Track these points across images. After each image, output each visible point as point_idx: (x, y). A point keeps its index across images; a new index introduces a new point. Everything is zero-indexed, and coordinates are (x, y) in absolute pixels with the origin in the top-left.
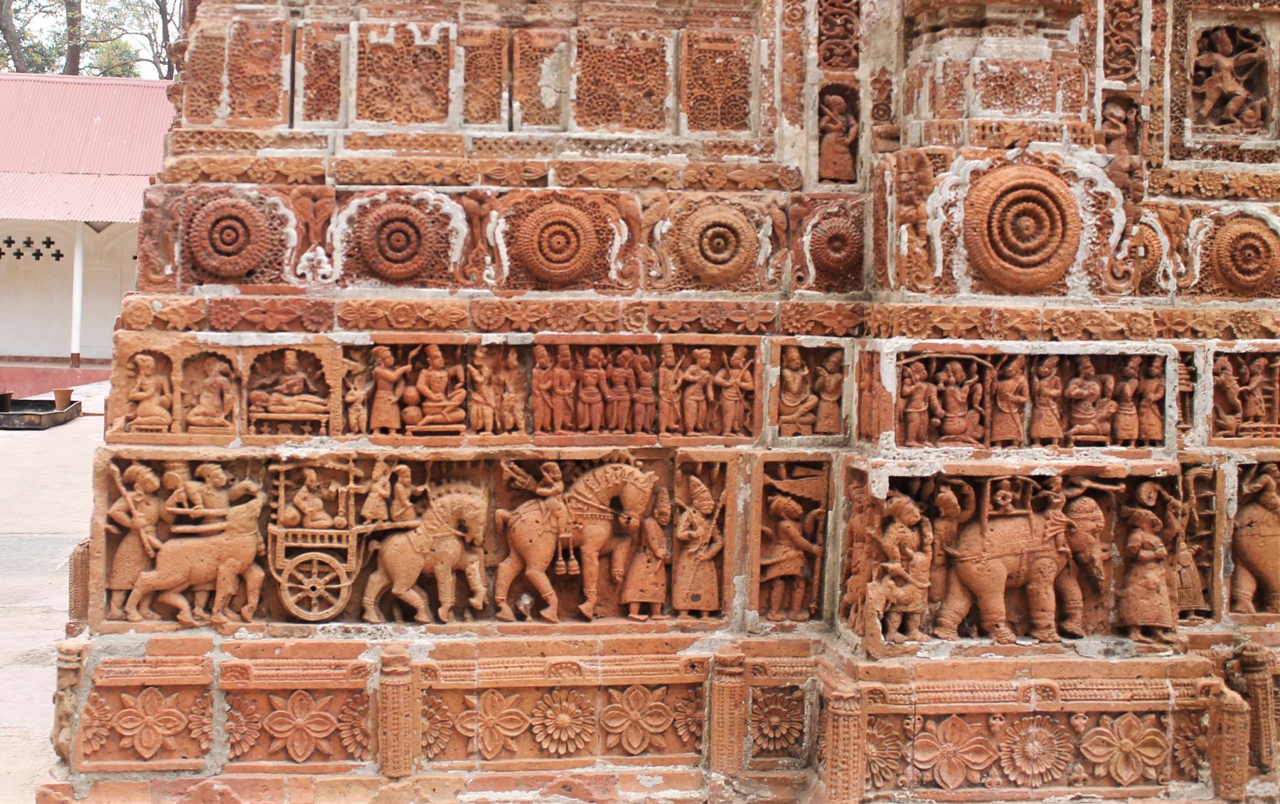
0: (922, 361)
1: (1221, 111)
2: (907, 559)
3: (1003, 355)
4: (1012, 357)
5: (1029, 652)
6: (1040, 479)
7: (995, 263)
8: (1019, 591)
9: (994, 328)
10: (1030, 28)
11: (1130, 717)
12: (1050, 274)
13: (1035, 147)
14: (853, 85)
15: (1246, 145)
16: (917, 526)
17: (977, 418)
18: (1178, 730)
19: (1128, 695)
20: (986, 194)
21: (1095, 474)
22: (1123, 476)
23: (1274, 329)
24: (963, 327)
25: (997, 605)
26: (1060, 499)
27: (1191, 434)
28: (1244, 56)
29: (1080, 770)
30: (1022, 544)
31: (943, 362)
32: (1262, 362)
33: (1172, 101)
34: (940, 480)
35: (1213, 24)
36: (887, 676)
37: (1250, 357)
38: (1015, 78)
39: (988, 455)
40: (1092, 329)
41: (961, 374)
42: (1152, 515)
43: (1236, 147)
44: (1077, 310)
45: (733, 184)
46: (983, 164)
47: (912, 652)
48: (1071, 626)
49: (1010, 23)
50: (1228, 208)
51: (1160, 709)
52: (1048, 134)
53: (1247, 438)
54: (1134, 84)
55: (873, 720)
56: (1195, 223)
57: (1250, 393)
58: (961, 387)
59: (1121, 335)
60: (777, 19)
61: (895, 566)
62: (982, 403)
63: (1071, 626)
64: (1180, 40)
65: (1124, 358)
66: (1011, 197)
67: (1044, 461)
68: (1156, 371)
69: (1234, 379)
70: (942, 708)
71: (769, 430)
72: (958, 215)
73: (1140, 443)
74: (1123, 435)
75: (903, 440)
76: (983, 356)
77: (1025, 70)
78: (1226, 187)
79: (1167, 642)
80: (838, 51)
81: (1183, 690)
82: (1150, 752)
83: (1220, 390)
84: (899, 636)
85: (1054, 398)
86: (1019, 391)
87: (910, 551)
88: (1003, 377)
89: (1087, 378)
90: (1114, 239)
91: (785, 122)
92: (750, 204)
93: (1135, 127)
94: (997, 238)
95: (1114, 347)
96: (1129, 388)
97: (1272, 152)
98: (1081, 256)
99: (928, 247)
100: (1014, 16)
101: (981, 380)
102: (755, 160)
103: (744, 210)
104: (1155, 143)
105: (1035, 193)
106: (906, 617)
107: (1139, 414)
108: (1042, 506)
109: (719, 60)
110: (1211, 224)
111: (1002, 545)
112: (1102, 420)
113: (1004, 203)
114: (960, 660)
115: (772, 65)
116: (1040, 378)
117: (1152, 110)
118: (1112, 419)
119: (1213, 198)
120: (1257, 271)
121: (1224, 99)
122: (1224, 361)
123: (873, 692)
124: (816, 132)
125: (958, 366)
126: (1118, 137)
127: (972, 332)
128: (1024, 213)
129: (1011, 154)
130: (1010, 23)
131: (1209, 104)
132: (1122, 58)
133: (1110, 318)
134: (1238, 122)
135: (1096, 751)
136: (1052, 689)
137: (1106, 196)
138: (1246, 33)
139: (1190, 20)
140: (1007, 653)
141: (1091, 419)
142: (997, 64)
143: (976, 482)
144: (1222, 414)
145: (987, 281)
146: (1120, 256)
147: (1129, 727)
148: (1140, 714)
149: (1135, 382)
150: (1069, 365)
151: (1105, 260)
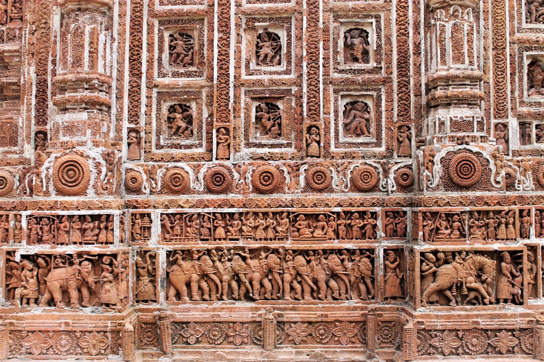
0: (34, 218)
1: (178, 132)
2: (27, 281)
3: (60, 215)
4: (63, 216)
5: (67, 312)
6: (71, 255)
7: (61, 186)
8: (65, 291)
9: (59, 207)
10: (81, 110)
11: (95, 333)
12: (79, 189)
13: (78, 148)
14: (45, 131)
15: (183, 143)
16: (31, 270)
17: (52, 236)
18: (112, 338)
19: (95, 325)
20: (57, 164)
21: (88, 253)
22: (96, 254)
23: (183, 205)
24: (48, 207)
25: (58, 296)
26: (78, 261)
27: (151, 241)
28: (185, 113)
29: (79, 350)
30: (63, 276)
31: (41, 218)
32: (178, 216)
33: (157, 130)
34: (37, 256)
35: (173, 104)
36: (18, 318)
37: (174, 215)
38: (73, 126)
39: (55, 248)
40: (91, 206)
41: (48, 222)
42: (108, 267)
43: (179, 144)
44: (91, 200)
45: (8, 164)
46: (59, 155)
47: (29, 311)
48: (83, 304)
49: (75, 109)
50: (171, 165)
51: (105, 330)
52: (83, 144)
53: (173, 242)
54: (138, 125)
55: (11, 332)
56: (159, 171)
57: (174, 227)
58: (49, 225)
59: (101, 208)
60: (25, 111)
61: (24, 283)
62: (54, 231)
63: (83, 304)
64: (159, 110)
65: (100, 216)
66: (65, 165)
67: (71, 249)
68: (111, 219)
69: (168, 222)
70: (33, 329)
71: (11, 241)
72: (51, 171)
73: (107, 243)
74: (100, 240)
75: (29, 243)
76: (54, 216)
77: (76, 124)
78: (173, 158)
79: (113, 309)
80: (41, 120)
81: (113, 324)
82: (102, 345)
83: (163, 226)
84: (26, 306)
85: (78, 229)
86: (65, 227)
87: (28, 278)
88: (61, 223)
89: (89, 222)
90: (102, 176)
91: (26, 143)
92: (12, 170)
93: (139, 139)
94: (61, 178)
95: (96, 212)
96: (102, 226)
97: (192, 145)
98: (92, 183)
99: (41, 182)
100: (75, 107)
101: (54, 224)
102: (17, 156)
103: (10, 172)
104: (148, 144)
105: (73, 163)
106: (28, 300)
107: (107, 233)
108: (71, 264)
109: (9, 125)
110: (165, 170)
111: (58, 276)
112: (93, 236)
113: (63, 167)
114: (45, 313)
115: (23, 126)
116: (73, 223)
117: (146, 133)
118: (97, 235)
119: (168, 161)
120: (180, 185)
121: (179, 128)
122: (165, 216)
123: (10, 323)
124: (33, 146)
125: (46, 219)
126: (133, 143)
127: (52, 208)
128: (69, 170)
129: (68, 151)
130: (75, 109)
131: (174, 130)
132: (134, 117)
133: (98, 203)
134: (183, 136)
135: (84, 344)
136: (68, 323)
137: (99, 163)
138: (185, 106)
139: (162, 103)
140: (60, 312)
141: (90, 235)
142: (67, 122)
143: (50, 256)
144: (166, 234)
145: (60, 192)
146: (104, 183)
147: (94, 336)
148: (98, 332)
149: (105, 223)
150: (82, 218)
151: (99, 184)
